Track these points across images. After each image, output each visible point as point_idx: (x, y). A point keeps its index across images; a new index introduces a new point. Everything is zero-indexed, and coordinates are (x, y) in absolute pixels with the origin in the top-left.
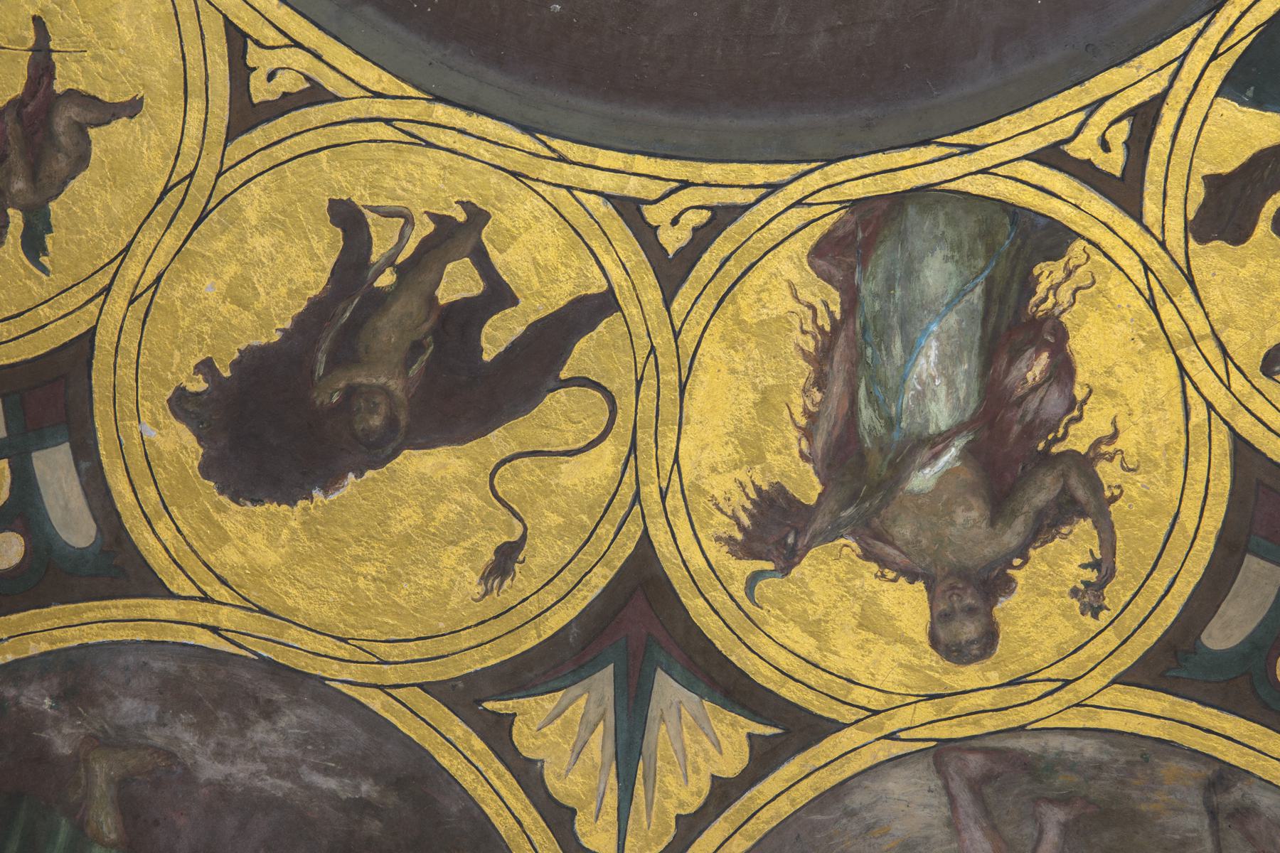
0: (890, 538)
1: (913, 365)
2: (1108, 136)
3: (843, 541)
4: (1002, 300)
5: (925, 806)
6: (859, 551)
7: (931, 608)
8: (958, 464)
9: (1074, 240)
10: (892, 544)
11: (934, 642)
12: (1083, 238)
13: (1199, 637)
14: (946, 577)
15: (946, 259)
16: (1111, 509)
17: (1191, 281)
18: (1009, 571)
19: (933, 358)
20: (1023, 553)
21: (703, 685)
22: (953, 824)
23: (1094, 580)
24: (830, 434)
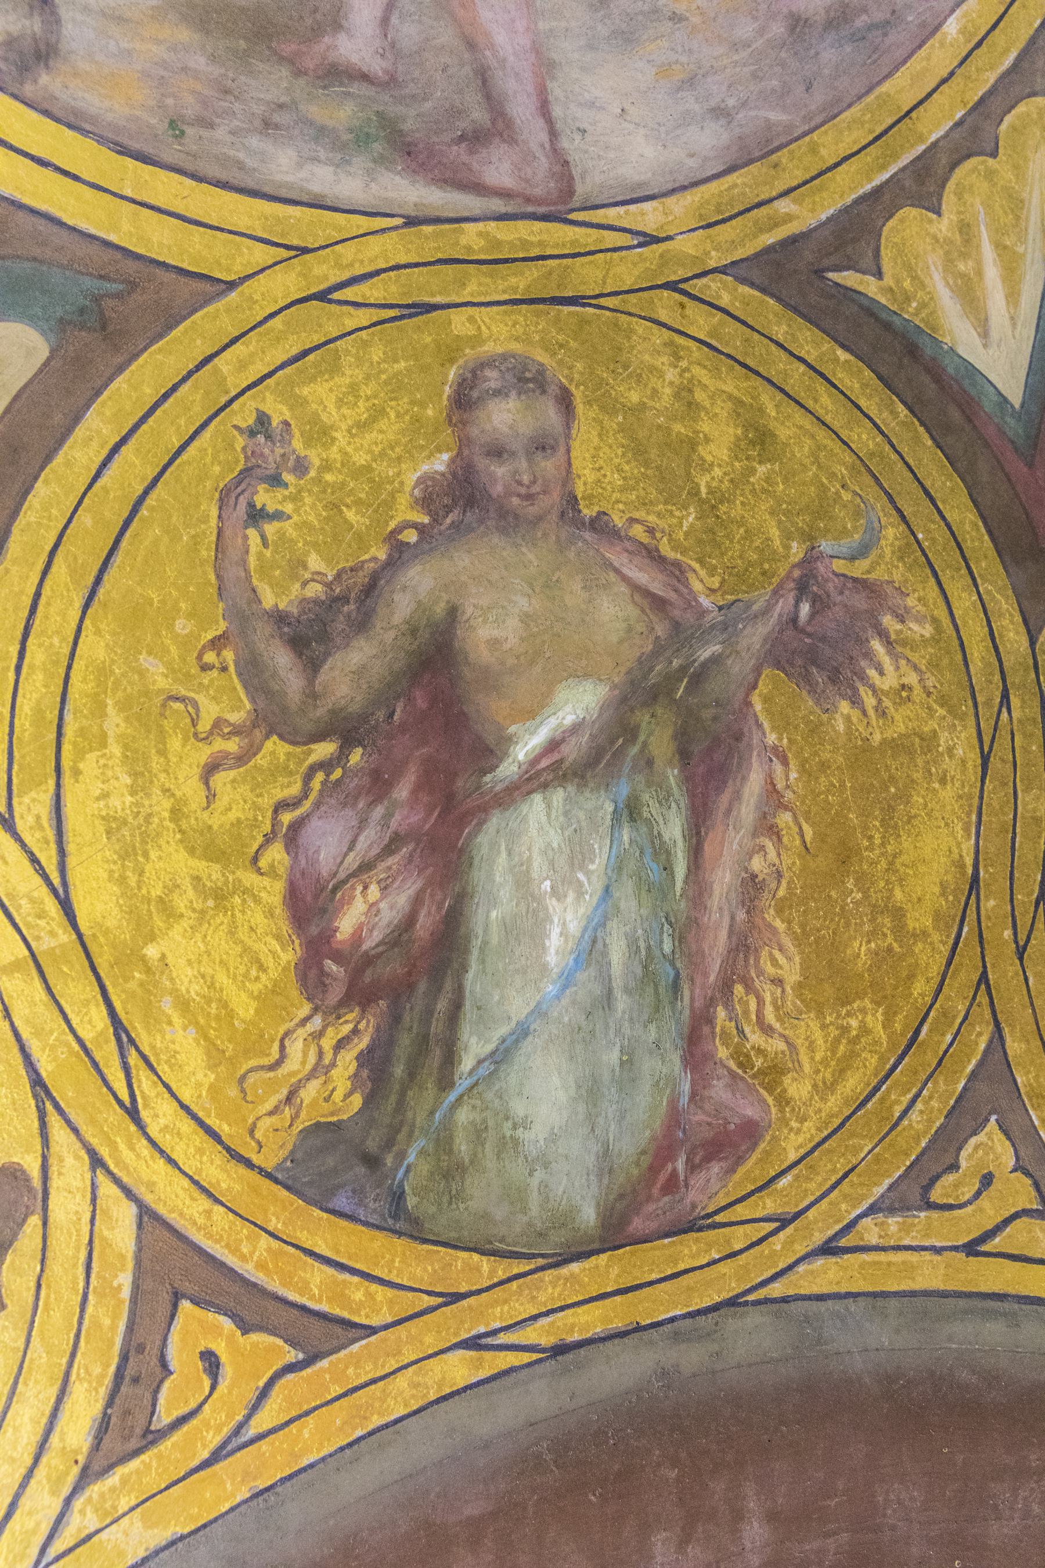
0: (637, 598)
1: (589, 920)
2: (207, 1383)
4: (423, 1042)
5: (591, 105)
8: (512, 729)
9: (279, 1167)
10: (636, 588)
11: (565, 402)
12: (261, 1171)
13: (53, 351)
14: (540, 518)
16: (222, 626)
17: (38, 1082)
18: (426, 520)
19: (555, 932)
20: (400, 554)
21: (951, 370)
22: (545, 67)
23: (261, 488)
24: (737, 796)
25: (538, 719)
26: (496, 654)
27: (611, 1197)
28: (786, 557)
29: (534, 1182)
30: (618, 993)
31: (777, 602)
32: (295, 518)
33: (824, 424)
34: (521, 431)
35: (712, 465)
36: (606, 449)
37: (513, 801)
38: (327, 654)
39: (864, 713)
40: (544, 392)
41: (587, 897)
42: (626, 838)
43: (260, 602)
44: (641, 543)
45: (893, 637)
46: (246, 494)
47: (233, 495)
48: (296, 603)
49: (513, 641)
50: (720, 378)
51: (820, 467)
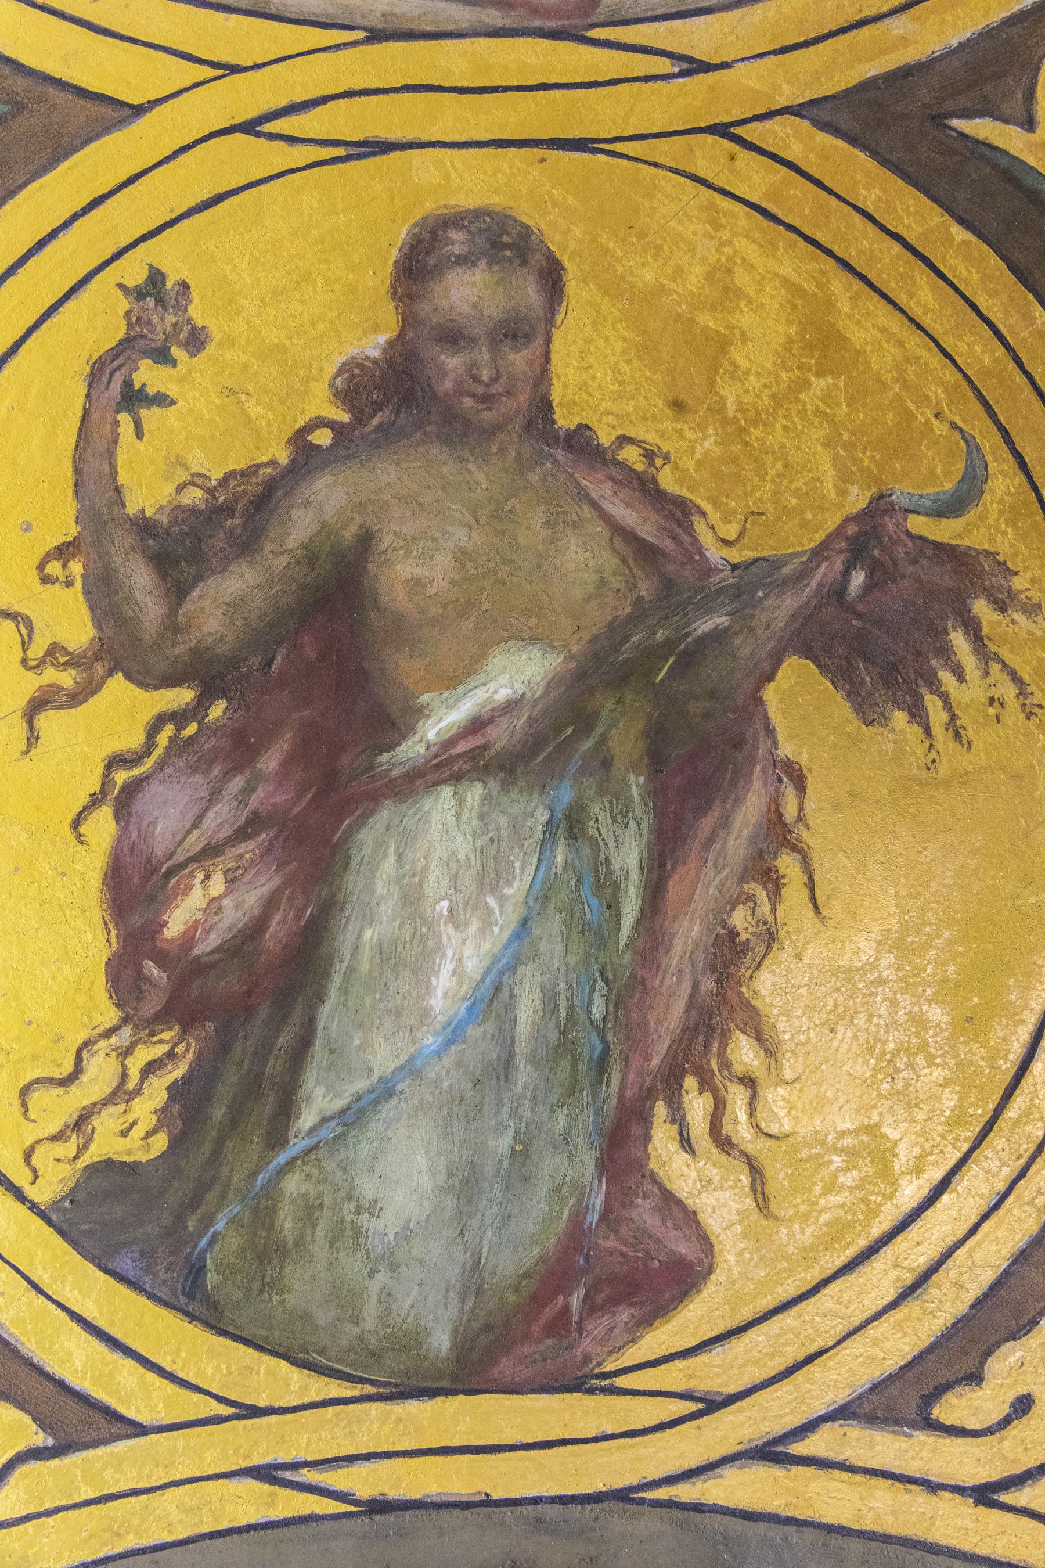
0: (618, 543)
1: (496, 959)
3: (735, 556)
4: (254, 1084)
6: (700, 527)
7: (547, 359)
8: (426, 698)
9: (55, 1205)
10: (618, 530)
11: (552, 279)
12: (33, 1207)
14: (498, 428)
15: (374, 1209)
16: (74, 530)
18: (346, 418)
19: (446, 969)
20: (305, 457)
23: (145, 364)
24: (725, 822)
25: (461, 689)
26: (416, 599)
27: (476, 1326)
28: (840, 506)
29: (374, 1287)
30: (521, 1061)
31: (818, 566)
32: (181, 403)
33: (919, 327)
34: (487, 312)
35: (747, 373)
36: (601, 344)
37: (413, 792)
38: (198, 579)
39: (928, 732)
40: (524, 262)
41: (496, 930)
42: (560, 859)
43: (124, 506)
44: (634, 471)
45: (985, 631)
46: (123, 370)
47: (108, 371)
48: (167, 510)
49: (440, 585)
50: (774, 256)
51: (905, 386)
